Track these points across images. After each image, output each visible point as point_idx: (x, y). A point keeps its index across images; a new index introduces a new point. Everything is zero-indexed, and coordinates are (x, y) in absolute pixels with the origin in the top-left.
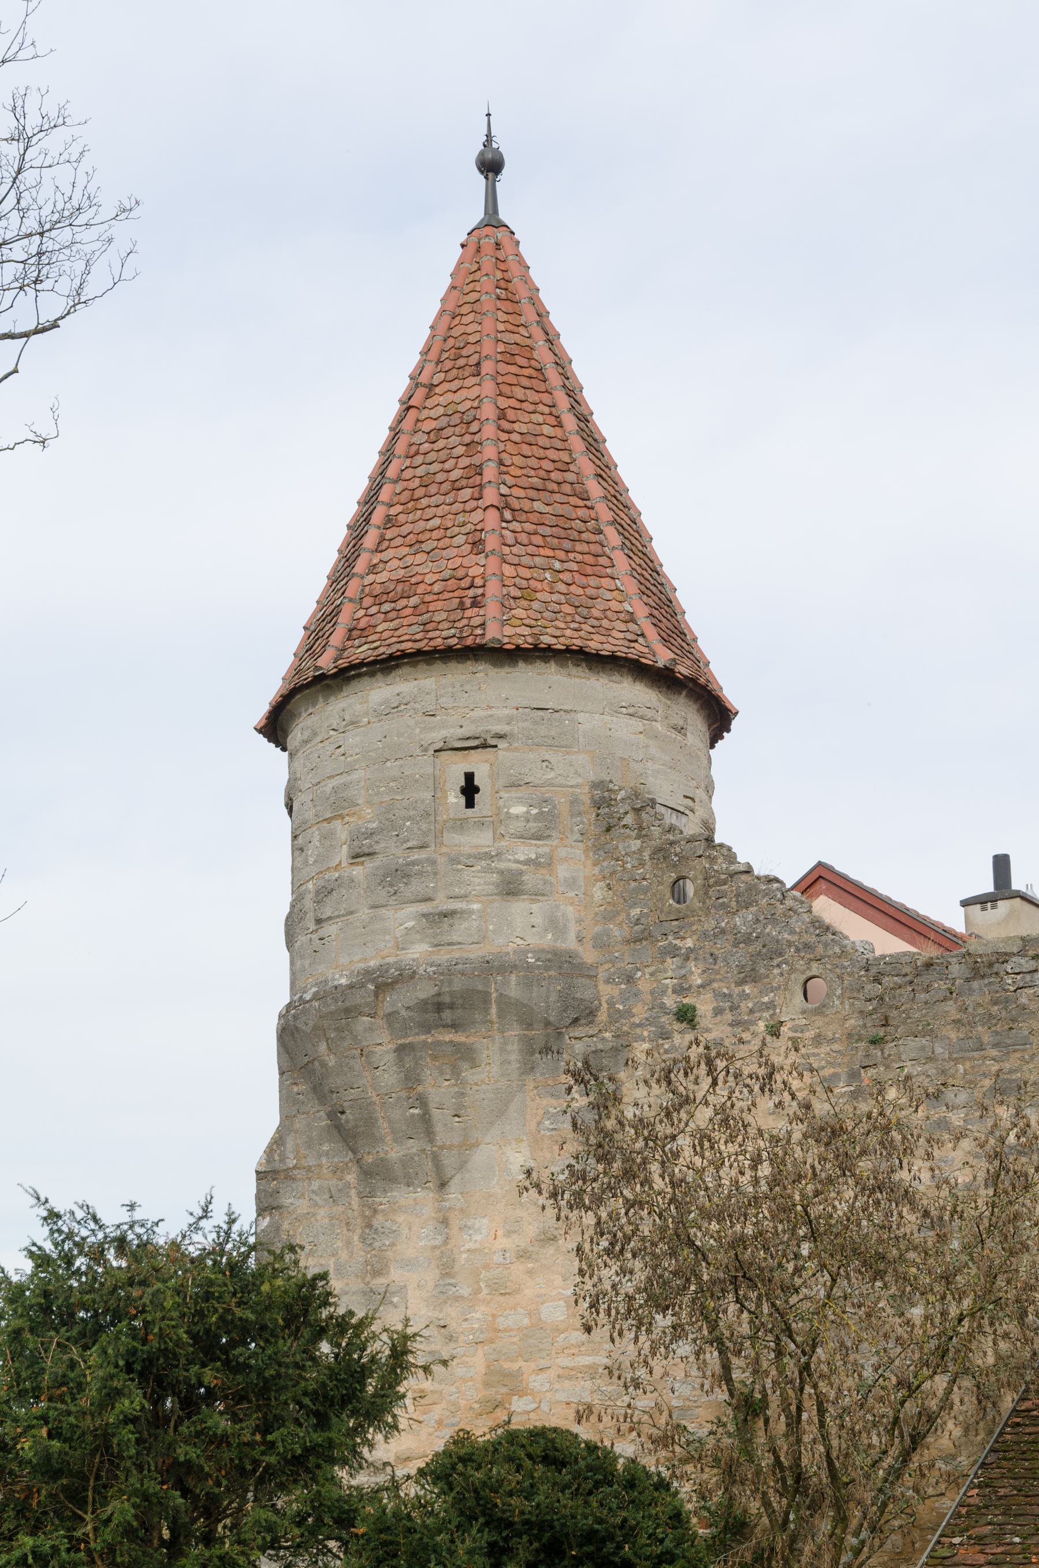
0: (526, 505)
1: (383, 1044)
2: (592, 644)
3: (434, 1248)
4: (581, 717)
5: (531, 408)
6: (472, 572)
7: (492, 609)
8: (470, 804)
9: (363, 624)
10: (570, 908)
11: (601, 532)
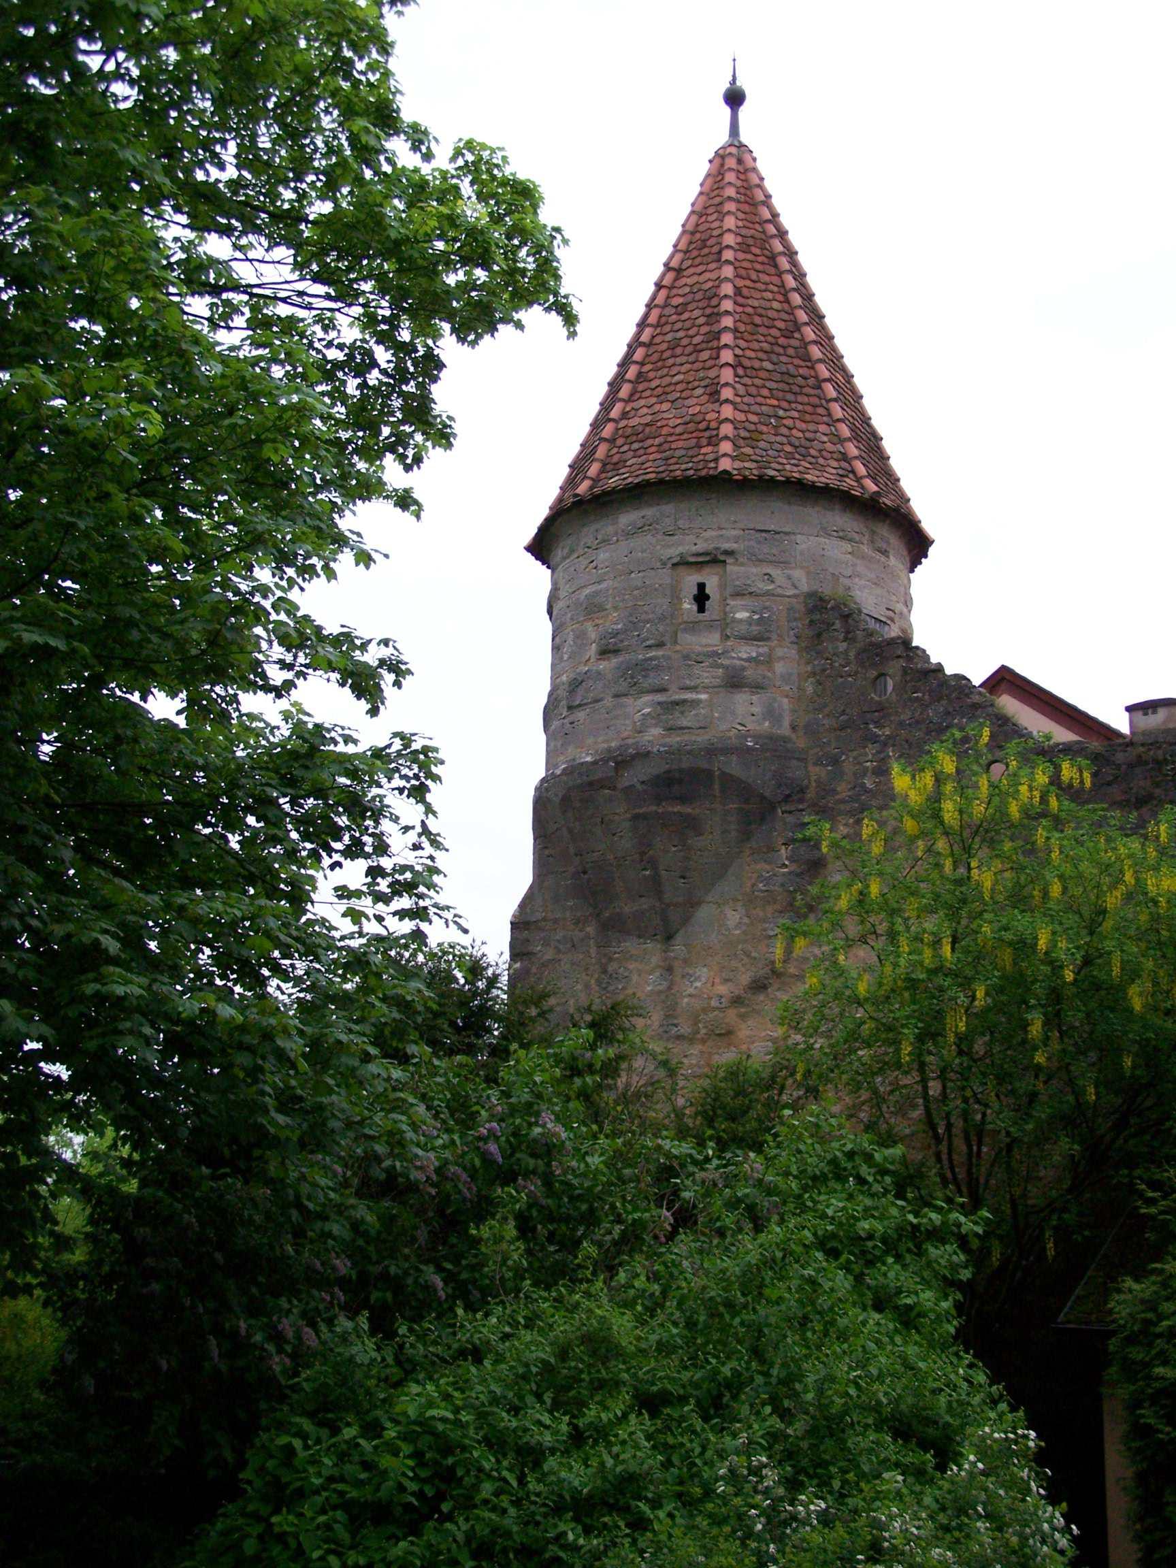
0: (757, 364)
1: (620, 812)
2: (809, 477)
3: (660, 992)
4: (799, 538)
5: (763, 287)
6: (708, 417)
7: (726, 447)
8: (701, 609)
9: (615, 459)
10: (786, 700)
11: (820, 387)
